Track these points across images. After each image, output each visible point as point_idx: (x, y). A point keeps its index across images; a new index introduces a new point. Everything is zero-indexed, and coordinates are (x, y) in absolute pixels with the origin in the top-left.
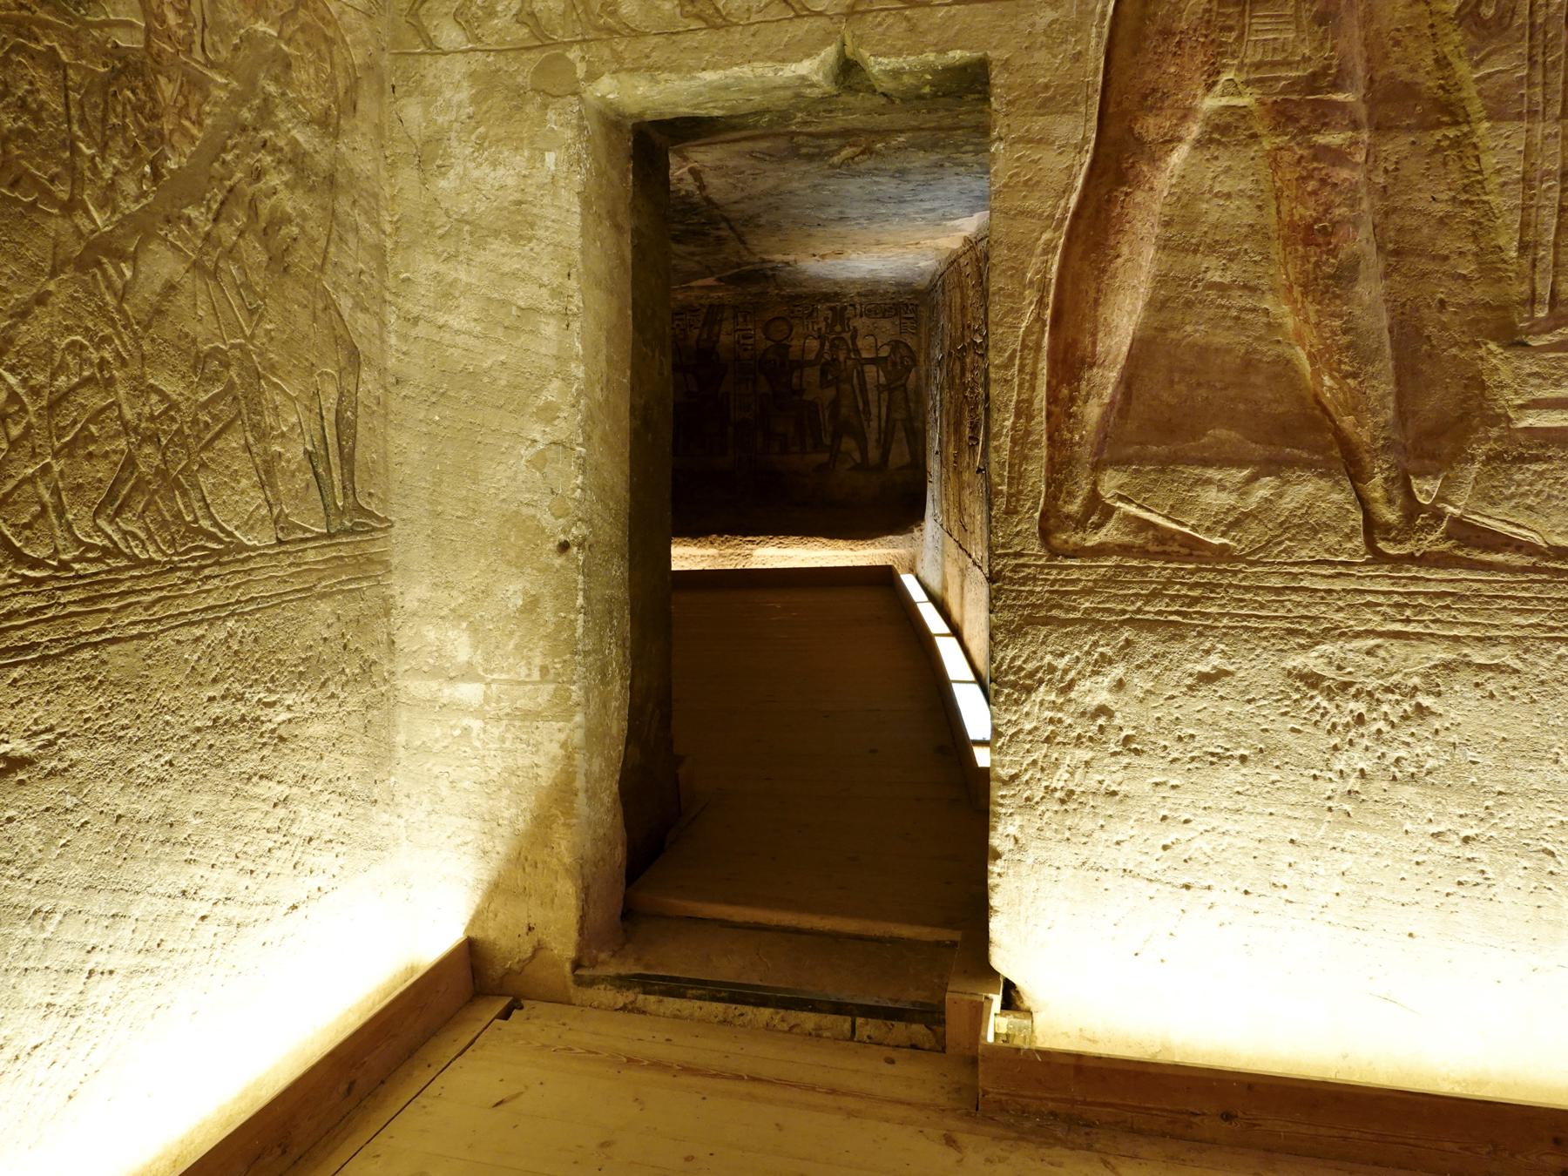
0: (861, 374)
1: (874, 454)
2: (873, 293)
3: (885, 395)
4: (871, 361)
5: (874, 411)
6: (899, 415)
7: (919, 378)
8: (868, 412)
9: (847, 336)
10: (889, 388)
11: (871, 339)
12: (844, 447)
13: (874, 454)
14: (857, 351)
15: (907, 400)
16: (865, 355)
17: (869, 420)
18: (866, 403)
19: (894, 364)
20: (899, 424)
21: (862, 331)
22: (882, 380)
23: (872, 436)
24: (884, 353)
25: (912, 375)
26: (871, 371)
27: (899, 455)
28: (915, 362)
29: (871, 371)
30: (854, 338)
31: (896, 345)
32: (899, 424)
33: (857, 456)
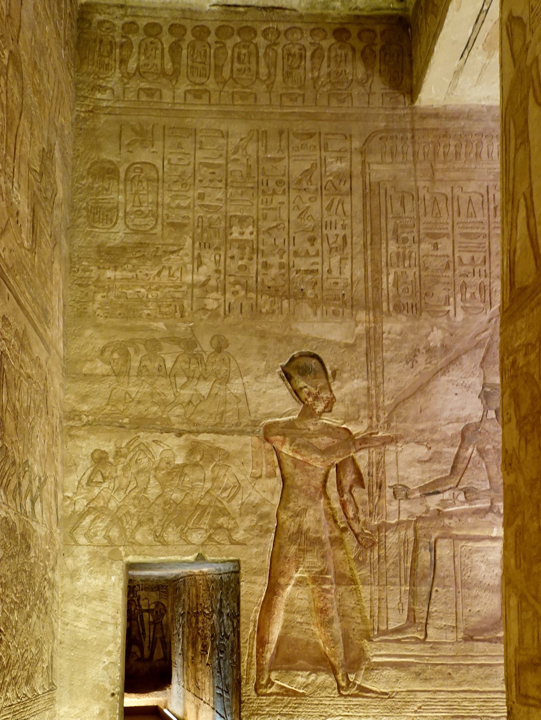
0: (142, 617)
1: (147, 653)
2: (148, 580)
3: (152, 626)
4: (148, 611)
5: (147, 633)
6: (159, 635)
7: (168, 618)
8: (144, 634)
9: (135, 599)
10: (154, 623)
11: (146, 601)
12: (132, 650)
13: (147, 653)
14: (140, 606)
15: (162, 628)
16: (143, 608)
17: (145, 637)
18: (144, 630)
19: (157, 612)
20: (158, 640)
21: (142, 597)
22: (151, 619)
23: (146, 644)
24: (152, 607)
25: (165, 618)
26: (146, 615)
27: (158, 654)
28: (166, 611)
29: (146, 615)
30: (139, 600)
31: (157, 604)
32: (158, 640)
33: (139, 654)
